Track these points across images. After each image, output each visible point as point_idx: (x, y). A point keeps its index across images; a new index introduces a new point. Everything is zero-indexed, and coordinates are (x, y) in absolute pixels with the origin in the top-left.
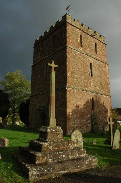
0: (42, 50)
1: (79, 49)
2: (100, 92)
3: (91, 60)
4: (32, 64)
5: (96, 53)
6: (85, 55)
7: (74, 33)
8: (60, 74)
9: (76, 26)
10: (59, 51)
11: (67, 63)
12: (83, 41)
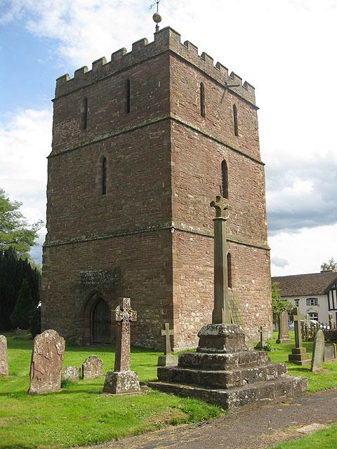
0: (86, 114)
1: (198, 125)
3: (225, 152)
4: (49, 150)
5: (236, 135)
8: (149, 191)
9: (191, 61)
10: (146, 125)
11: (172, 164)
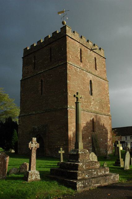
0: (35, 63)
1: (79, 66)
2: (100, 112)
3: (91, 77)
6: (85, 72)
7: (74, 48)
9: (76, 39)
10: (58, 66)
11: (68, 81)
12: (82, 56)
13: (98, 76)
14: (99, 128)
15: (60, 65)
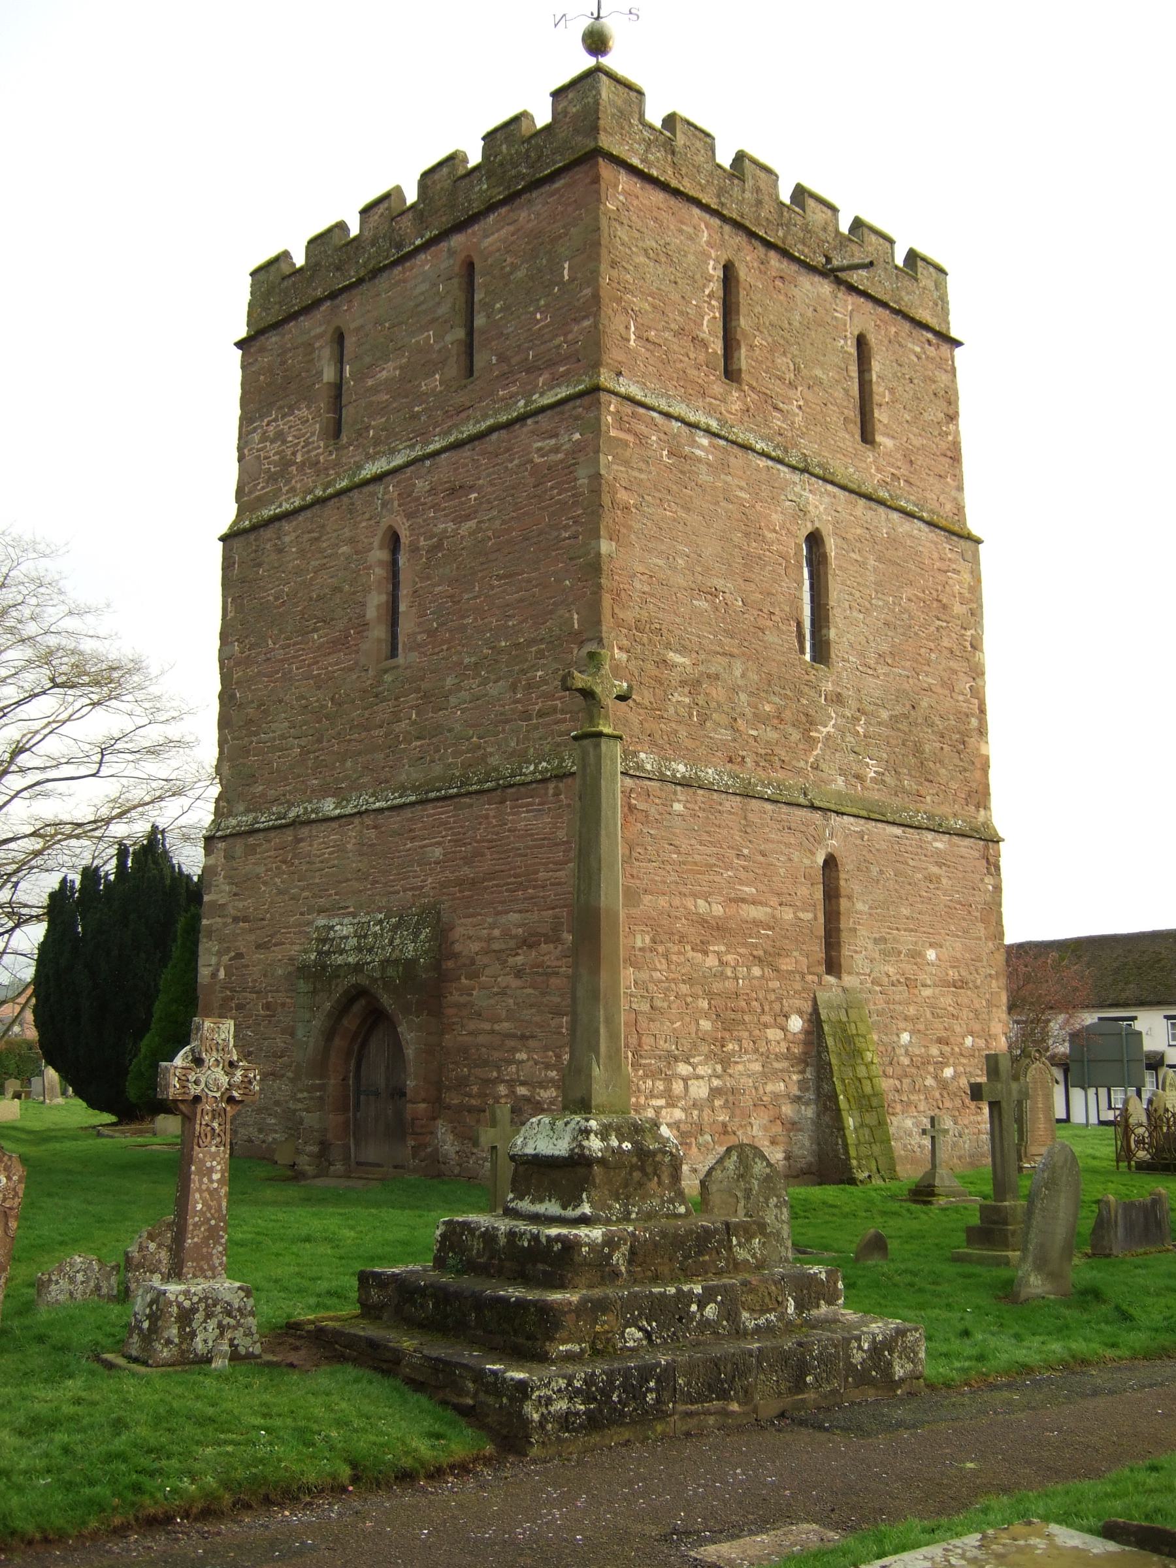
0: (338, 388)
1: (710, 411)
2: (897, 802)
3: (821, 506)
4: (226, 514)
5: (867, 436)
6: (763, 463)
7: (664, 255)
8: (532, 642)
9: (687, 186)
10: (522, 419)
11: (606, 547)
12: (744, 322)
13: (883, 494)
14: (883, 940)
15: (543, 410)
